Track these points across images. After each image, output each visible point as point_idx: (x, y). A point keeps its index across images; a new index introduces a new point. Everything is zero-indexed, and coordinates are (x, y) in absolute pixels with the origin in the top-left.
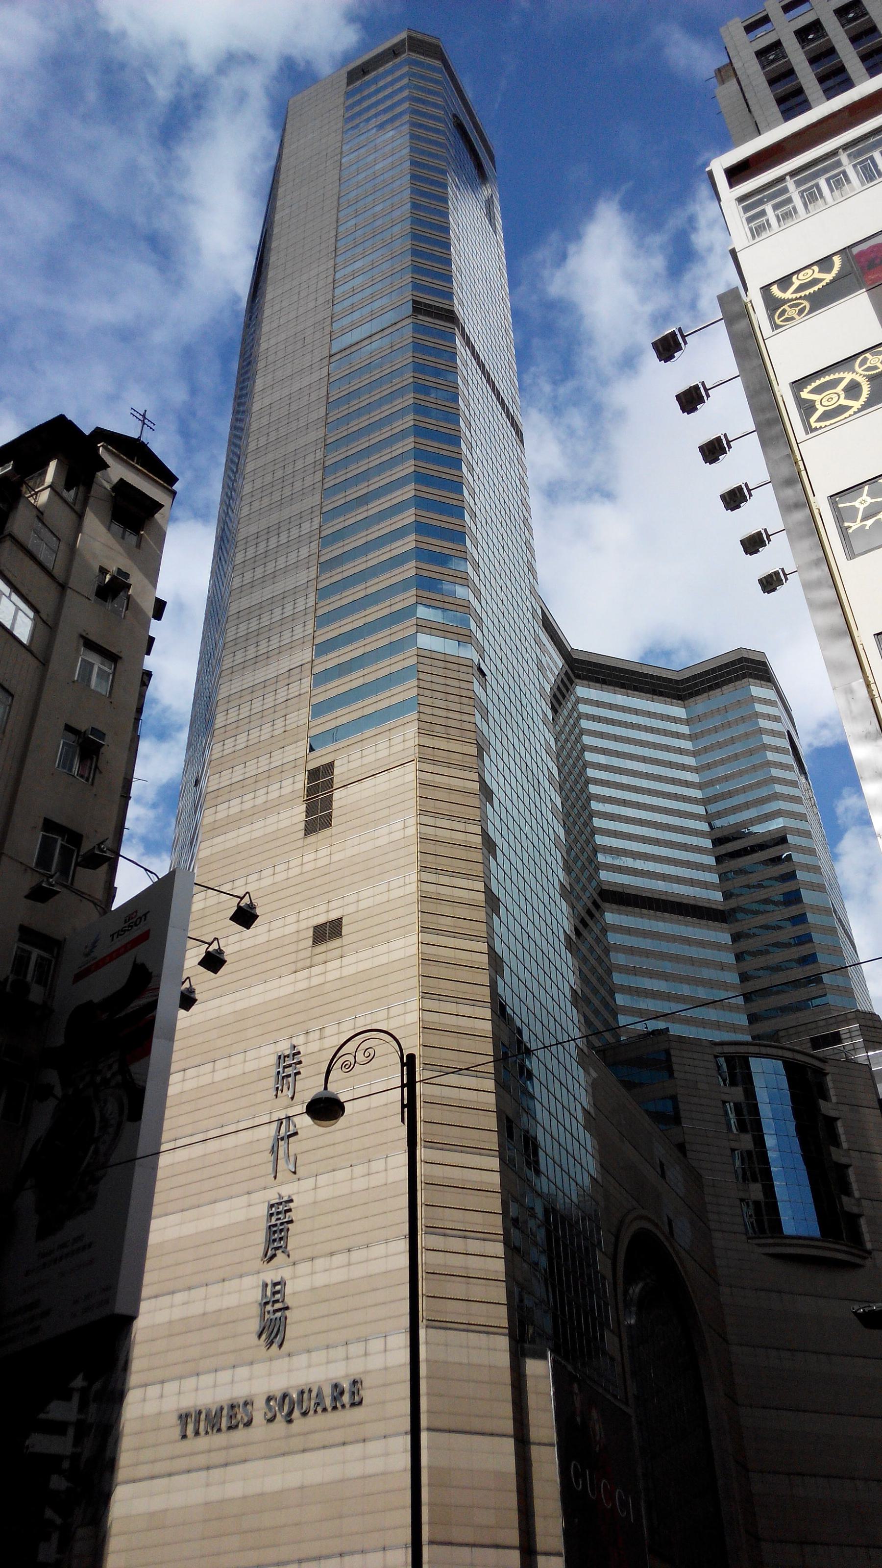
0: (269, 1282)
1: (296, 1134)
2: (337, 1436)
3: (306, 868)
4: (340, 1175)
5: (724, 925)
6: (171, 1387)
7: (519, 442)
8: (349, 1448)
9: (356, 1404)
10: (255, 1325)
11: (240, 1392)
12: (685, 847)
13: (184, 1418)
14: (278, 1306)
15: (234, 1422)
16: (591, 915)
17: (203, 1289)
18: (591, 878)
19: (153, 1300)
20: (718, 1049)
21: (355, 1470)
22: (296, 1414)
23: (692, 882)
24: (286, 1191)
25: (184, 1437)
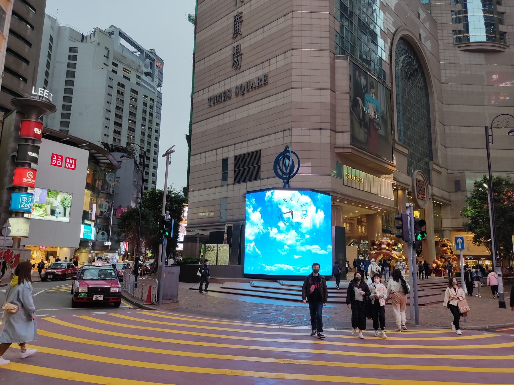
0: (235, 46)
2: (260, 96)
9: (266, 84)
10: (230, 64)
11: (227, 87)
13: (210, 99)
21: (266, 107)
22: (245, 92)
25: (210, 106)
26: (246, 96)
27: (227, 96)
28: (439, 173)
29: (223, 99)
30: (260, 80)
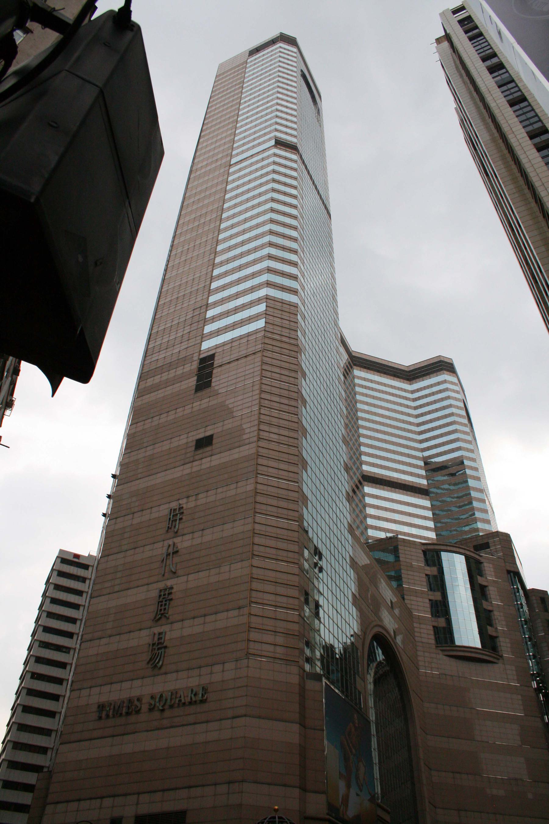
1: (177, 552)
3: (195, 409)
4: (201, 574)
5: (427, 497)
6: (95, 690)
7: (329, 217)
8: (197, 726)
11: (136, 693)
13: (101, 707)
14: (159, 646)
15: (130, 710)
16: (358, 488)
17: (118, 637)
18: (358, 469)
19: (89, 642)
20: (425, 547)
22: (166, 707)
23: (411, 474)
24: (169, 583)
25: (100, 718)
26: (167, 713)
27: (133, 707)
29: (124, 711)
30: (194, 693)
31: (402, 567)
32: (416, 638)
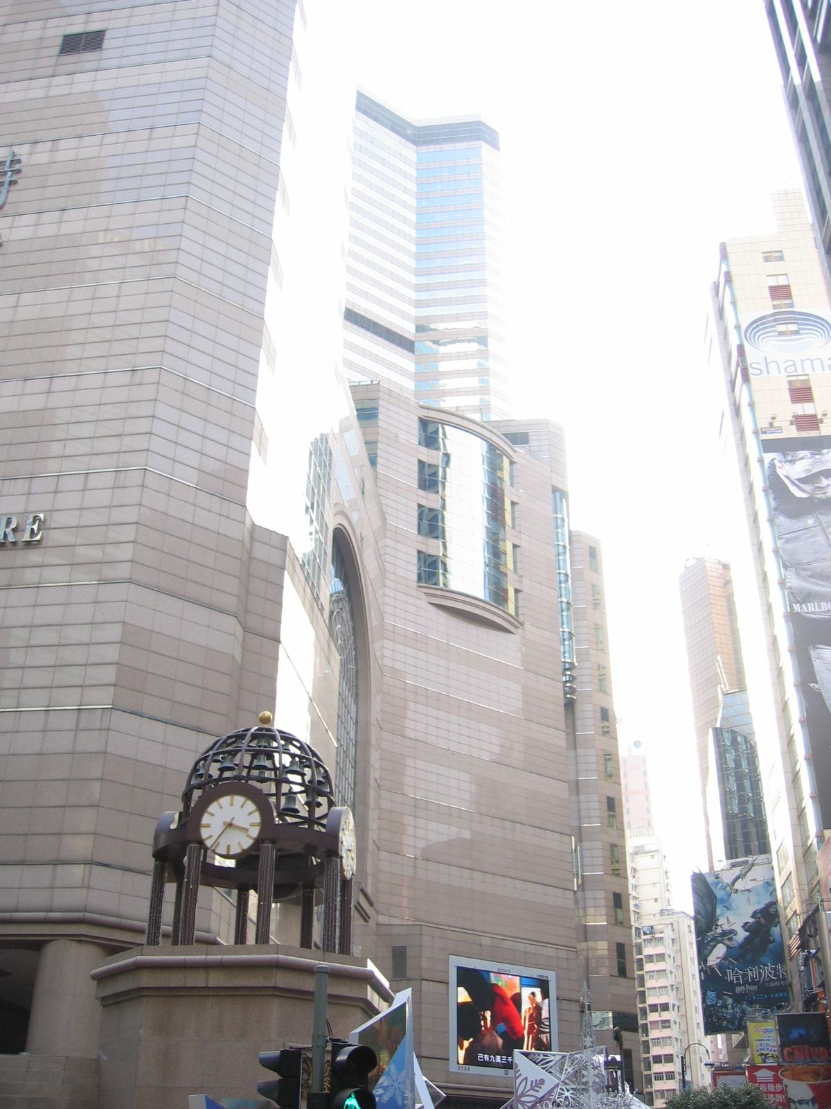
5: (411, 354)
12: (392, 275)
20: (424, 413)
23: (391, 308)
28: (366, 917)
31: (380, 437)
32: (387, 565)
